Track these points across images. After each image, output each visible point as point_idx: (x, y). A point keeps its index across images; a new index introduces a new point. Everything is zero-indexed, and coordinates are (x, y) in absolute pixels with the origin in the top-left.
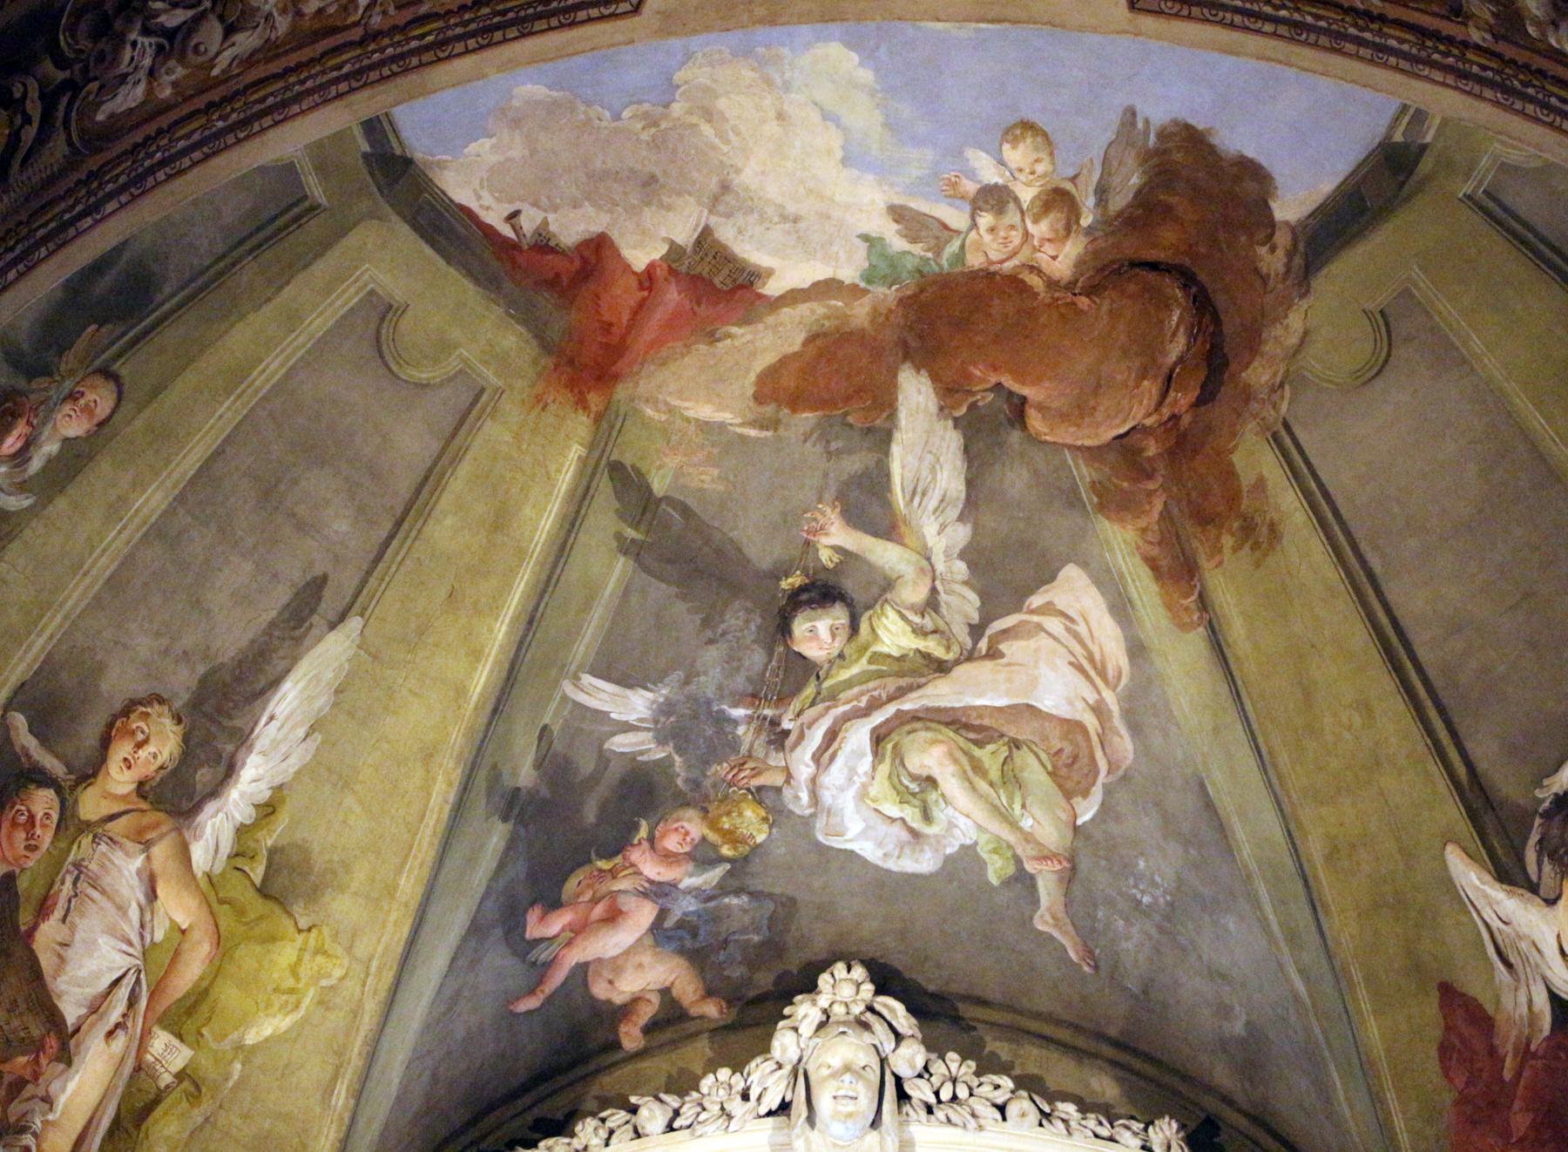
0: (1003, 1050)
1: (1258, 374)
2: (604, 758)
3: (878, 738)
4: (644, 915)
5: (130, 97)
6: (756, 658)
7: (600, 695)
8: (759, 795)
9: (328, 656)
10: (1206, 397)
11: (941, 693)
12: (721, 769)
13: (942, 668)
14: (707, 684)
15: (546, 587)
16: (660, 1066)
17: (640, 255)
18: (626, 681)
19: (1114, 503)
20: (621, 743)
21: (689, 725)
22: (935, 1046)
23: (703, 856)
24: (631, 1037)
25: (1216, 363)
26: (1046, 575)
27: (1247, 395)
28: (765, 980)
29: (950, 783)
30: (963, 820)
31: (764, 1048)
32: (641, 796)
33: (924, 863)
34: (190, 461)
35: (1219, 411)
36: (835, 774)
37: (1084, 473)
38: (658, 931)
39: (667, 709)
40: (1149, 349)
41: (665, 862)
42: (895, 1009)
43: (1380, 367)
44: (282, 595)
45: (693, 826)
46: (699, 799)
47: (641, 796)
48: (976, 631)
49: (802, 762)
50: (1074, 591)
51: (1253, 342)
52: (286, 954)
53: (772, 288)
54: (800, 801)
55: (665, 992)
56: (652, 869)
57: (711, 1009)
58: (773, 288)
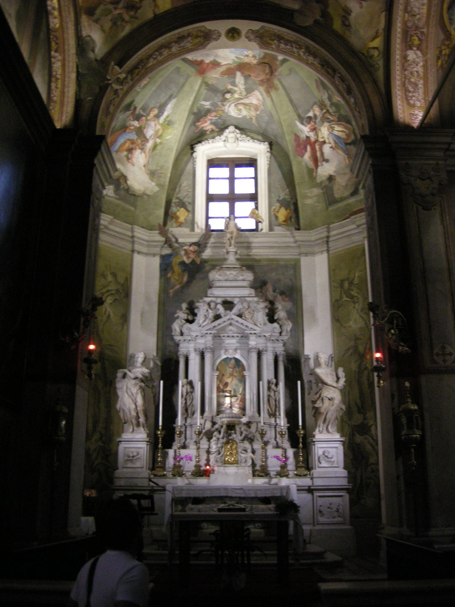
0: (249, 134)
1: (276, 74)
2: (204, 108)
3: (235, 105)
4: (209, 122)
5: (151, 64)
6: (221, 98)
7: (204, 103)
8: (221, 110)
9: (174, 101)
10: (271, 75)
11: (242, 101)
12: (217, 108)
13: (242, 99)
14: (215, 101)
15: (197, 94)
16: (211, 135)
17: (207, 61)
18: (206, 101)
19: (261, 85)
20: (206, 107)
21: (214, 105)
22: (242, 134)
23: (216, 116)
24: (208, 133)
25: (272, 72)
26: (253, 91)
27: (275, 76)
28: (223, 127)
29: (243, 109)
30: (244, 113)
31: (222, 134)
32: (208, 111)
33: (240, 117)
34: (158, 84)
35: (272, 77)
36: (230, 109)
37: (258, 82)
38: (211, 123)
39: (211, 103)
40: (264, 71)
41: (212, 117)
42: (237, 131)
43: (290, 74)
44: (167, 97)
45: (214, 114)
46: (215, 111)
47: (208, 111)
48: (246, 96)
49: (226, 107)
50: (256, 93)
51: (276, 70)
52: (170, 130)
53: (222, 64)
54: (226, 111)
55: (212, 129)
56: (210, 118)
57: (217, 130)
58: (222, 64)
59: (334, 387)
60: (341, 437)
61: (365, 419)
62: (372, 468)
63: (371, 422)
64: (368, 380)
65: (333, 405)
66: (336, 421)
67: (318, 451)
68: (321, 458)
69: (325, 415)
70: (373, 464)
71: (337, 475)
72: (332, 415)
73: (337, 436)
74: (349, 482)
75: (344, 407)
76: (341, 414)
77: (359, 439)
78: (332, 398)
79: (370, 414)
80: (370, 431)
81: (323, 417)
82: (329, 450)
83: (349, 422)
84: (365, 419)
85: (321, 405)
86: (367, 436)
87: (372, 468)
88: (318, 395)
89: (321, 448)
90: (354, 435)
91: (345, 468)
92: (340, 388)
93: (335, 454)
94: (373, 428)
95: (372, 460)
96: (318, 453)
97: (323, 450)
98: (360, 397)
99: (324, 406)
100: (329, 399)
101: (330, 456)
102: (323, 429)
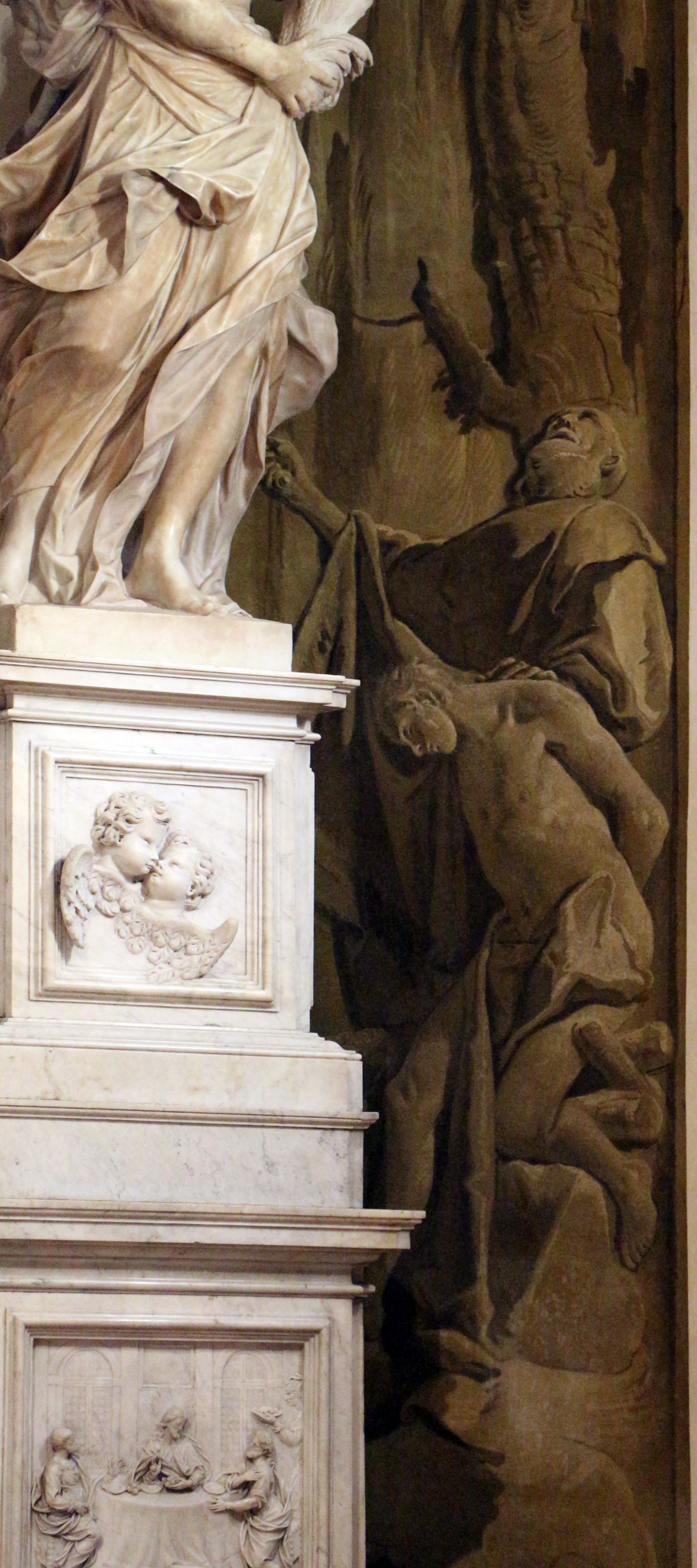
59: (249, 76)
60: (303, 662)
61: (528, 485)
62: (584, 1042)
64: (599, 48)
65: (220, 291)
66: (240, 475)
67: (40, 805)
68: (77, 890)
69: (121, 391)
70: (612, 997)
71: (254, 1102)
72: (213, 397)
73: (263, 653)
74: (377, 1189)
75: (322, 330)
77: (442, 703)
78: (216, 202)
79: (594, 443)
80: (588, 620)
81: (106, 410)
82: (186, 802)
83: (332, 513)
84: (528, 485)
85: (91, 269)
86: (555, 689)
87: (584, 1042)
88: (41, 152)
89: (68, 766)
92: (311, 96)
93: (230, 855)
95: (599, 946)
96: (40, 830)
97: (98, 792)
98: (484, 251)
99: (120, 288)
100: (189, 211)
101: (172, 877)
102: (88, 560)
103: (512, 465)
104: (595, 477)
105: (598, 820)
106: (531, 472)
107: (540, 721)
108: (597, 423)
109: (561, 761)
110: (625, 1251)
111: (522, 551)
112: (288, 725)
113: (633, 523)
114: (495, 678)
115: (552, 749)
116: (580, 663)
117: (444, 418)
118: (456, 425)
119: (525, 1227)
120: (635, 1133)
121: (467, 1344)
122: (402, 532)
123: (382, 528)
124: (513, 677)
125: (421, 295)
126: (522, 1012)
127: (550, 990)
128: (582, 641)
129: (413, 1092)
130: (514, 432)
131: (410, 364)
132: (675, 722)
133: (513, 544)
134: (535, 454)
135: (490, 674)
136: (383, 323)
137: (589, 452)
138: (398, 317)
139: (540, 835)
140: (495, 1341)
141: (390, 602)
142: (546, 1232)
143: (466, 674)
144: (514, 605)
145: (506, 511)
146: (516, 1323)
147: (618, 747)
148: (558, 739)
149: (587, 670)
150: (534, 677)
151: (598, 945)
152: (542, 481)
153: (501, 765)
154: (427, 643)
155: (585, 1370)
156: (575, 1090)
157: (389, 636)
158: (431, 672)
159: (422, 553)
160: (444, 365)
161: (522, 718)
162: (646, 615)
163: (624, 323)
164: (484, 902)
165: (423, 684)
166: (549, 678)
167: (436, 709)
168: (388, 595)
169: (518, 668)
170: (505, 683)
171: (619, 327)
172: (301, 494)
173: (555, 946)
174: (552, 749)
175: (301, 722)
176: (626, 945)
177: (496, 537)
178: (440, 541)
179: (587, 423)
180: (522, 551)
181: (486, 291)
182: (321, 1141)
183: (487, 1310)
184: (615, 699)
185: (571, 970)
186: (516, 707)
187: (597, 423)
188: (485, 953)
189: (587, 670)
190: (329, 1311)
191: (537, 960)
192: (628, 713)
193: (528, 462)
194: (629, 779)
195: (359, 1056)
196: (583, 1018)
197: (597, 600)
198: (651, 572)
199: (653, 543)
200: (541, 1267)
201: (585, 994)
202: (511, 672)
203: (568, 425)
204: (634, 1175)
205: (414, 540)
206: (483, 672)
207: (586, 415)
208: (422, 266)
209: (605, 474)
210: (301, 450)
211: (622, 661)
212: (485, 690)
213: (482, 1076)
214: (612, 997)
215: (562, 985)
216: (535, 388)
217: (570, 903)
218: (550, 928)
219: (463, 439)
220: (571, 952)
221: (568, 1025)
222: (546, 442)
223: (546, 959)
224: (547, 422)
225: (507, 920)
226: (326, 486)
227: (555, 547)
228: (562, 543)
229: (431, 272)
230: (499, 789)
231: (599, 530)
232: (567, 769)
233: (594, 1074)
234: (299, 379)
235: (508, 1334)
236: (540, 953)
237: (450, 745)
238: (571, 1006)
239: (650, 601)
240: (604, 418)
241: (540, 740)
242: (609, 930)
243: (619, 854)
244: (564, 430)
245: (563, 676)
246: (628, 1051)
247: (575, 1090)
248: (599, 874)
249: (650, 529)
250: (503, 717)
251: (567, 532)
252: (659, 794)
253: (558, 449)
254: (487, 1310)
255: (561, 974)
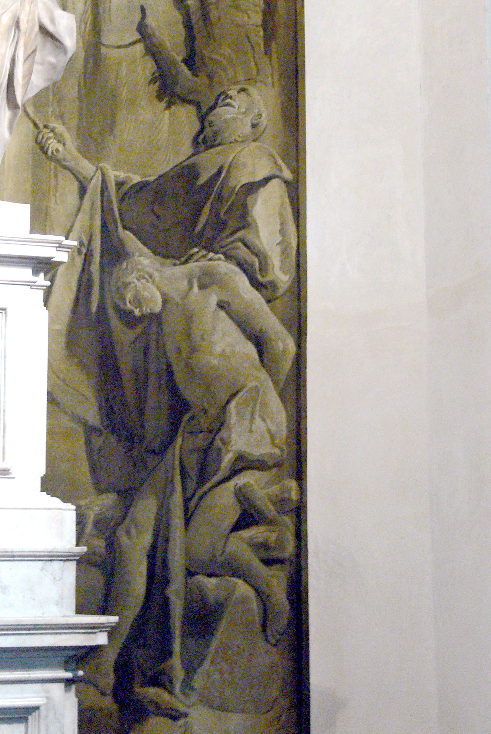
63: (252, 162)
70: (259, 465)
76: (38, 82)
79: (248, 107)
80: (243, 219)
84: (205, 139)
86: (224, 267)
90: (114, 254)
91: (50, 485)
94: (266, 210)
103: (197, 126)
104: (248, 129)
105: (251, 349)
106: (208, 129)
107: (214, 287)
108: (248, 95)
109: (227, 313)
110: (269, 633)
111: (201, 181)
112: (25, 273)
113: (271, 155)
114: (186, 262)
115: (221, 306)
116: (238, 248)
117: (156, 101)
118: (163, 105)
119: (203, 619)
120: (276, 554)
121: (166, 696)
122: (129, 175)
123: (117, 173)
124: (197, 261)
125: (142, 28)
126: (202, 479)
127: (220, 461)
128: (239, 234)
129: (133, 531)
130: (198, 105)
131: (132, 69)
132: (299, 282)
133: (197, 175)
134: (211, 118)
135: (183, 259)
136: (119, 47)
137: (244, 113)
138: (128, 42)
139: (215, 362)
140: (184, 693)
141: (122, 220)
142: (218, 620)
143: (168, 261)
144: (198, 213)
145: (193, 155)
146: (198, 682)
147: (263, 301)
148: (225, 297)
149: (243, 252)
150: (210, 260)
151: (251, 431)
152: (215, 134)
153: (189, 318)
154: (145, 244)
155: (243, 711)
156: (237, 527)
157: (120, 240)
158: (145, 262)
159: (141, 187)
160: (155, 68)
161: (202, 287)
162: (281, 214)
163: (265, 30)
164: (179, 407)
165: (142, 270)
166: (219, 259)
167: (149, 285)
168: (121, 215)
169: (200, 254)
170: (191, 265)
171: (262, 33)
172: (68, 157)
173: (223, 434)
174: (221, 306)
175: (36, 272)
176: (269, 431)
177: (187, 173)
178: (152, 178)
179: (243, 95)
180: (201, 181)
181: (181, 20)
182: (42, 569)
183: (179, 674)
184: (260, 269)
185: (234, 449)
186: (199, 278)
187: (248, 95)
188: (179, 441)
189: (243, 252)
190: (48, 692)
191: (212, 443)
192: (268, 278)
193: (206, 124)
194: (270, 322)
195: (74, 507)
196: (241, 480)
197: (249, 207)
198: (284, 186)
199: (284, 167)
200: (215, 643)
201: (243, 464)
202: (196, 258)
203: (231, 98)
204: (275, 581)
205: (137, 179)
206: (178, 259)
207: (242, 90)
208: (143, 10)
209: (254, 126)
210: (69, 130)
211: (266, 246)
212: (180, 271)
213: (178, 521)
214: (259, 465)
215: (227, 459)
216: (210, 77)
217: (232, 406)
218: (220, 423)
219: (167, 112)
220: (234, 436)
221: (231, 485)
222: (217, 110)
223: (218, 442)
224: (217, 99)
225: (193, 418)
226: (84, 151)
227: (223, 175)
228: (228, 172)
229: (148, 12)
230: (188, 334)
231: (250, 162)
232: (231, 318)
233: (247, 518)
234: (53, 60)
235: (192, 689)
236: (213, 440)
237: (158, 308)
238: (234, 473)
239: (282, 204)
240: (254, 91)
241: (214, 300)
242: (258, 421)
243: (264, 371)
244: (228, 101)
245: (228, 257)
246: (271, 501)
247: (237, 527)
248: (252, 384)
249: (283, 159)
250: (191, 288)
251: (230, 166)
252: (289, 329)
253: (224, 113)
254: (179, 674)
255: (229, 451)
